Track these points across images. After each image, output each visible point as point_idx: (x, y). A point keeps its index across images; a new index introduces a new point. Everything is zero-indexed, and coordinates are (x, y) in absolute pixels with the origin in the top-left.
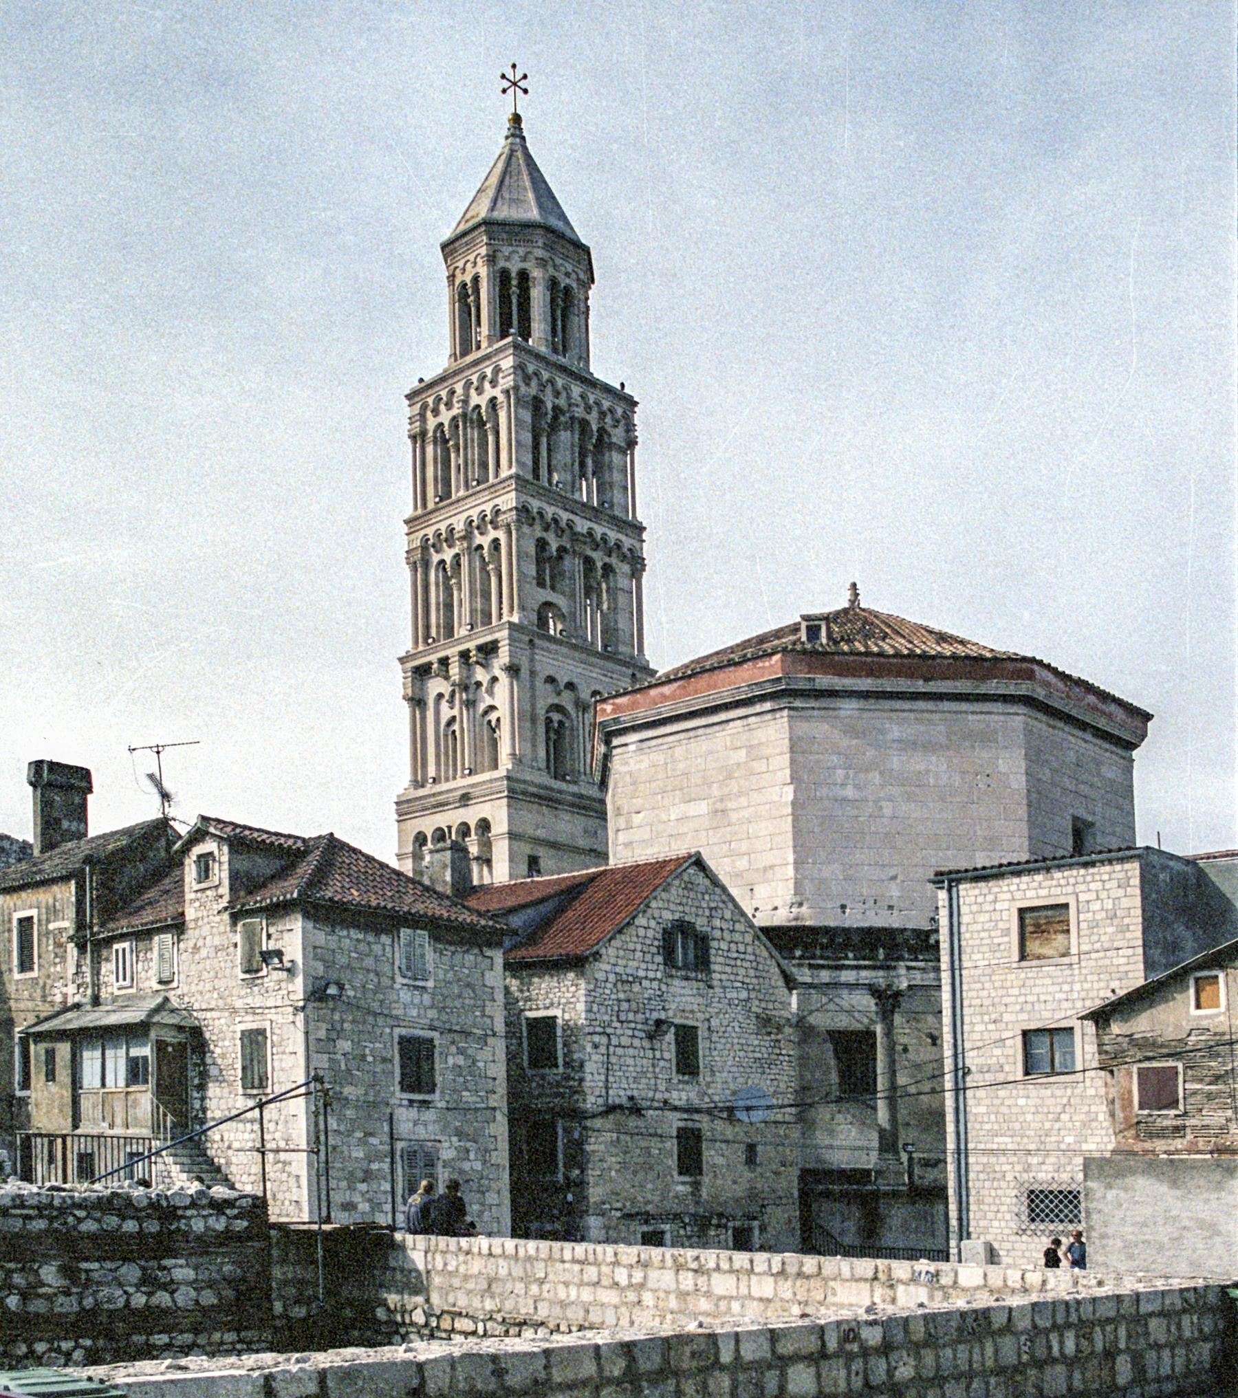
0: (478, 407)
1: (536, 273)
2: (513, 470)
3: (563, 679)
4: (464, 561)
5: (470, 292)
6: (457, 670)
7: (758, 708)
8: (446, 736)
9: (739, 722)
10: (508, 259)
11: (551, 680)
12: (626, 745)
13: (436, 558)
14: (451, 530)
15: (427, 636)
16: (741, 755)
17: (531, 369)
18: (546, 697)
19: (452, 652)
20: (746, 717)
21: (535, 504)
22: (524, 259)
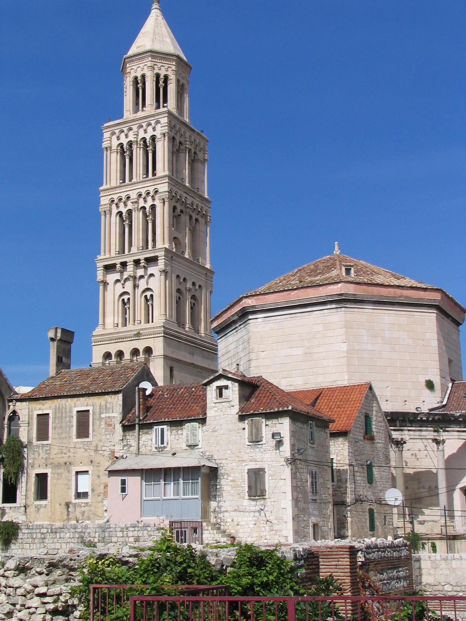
2: (167, 173)
6: (132, 269)
8: (118, 300)
13: (115, 211)
16: (320, 328)
19: (130, 260)
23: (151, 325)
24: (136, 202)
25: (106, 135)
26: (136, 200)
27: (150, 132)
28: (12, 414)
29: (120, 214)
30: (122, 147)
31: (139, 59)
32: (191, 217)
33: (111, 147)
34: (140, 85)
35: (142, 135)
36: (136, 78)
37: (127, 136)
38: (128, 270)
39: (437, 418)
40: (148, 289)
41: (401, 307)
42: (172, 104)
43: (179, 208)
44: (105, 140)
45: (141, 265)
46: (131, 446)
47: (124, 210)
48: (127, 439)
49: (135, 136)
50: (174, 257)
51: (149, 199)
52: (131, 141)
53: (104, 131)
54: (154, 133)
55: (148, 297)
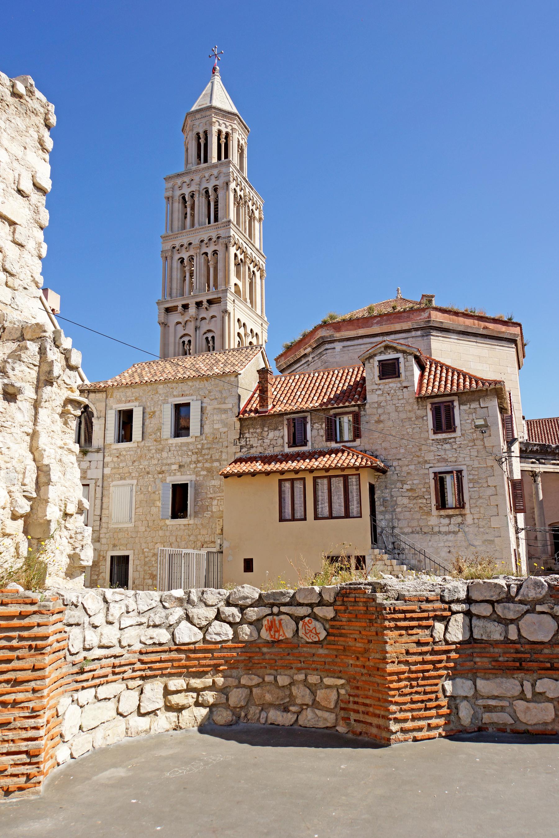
5: (201, 136)
7: (413, 333)
11: (239, 320)
15: (171, 295)
20: (407, 338)
27: (213, 182)
29: (182, 260)
30: (184, 198)
32: (249, 268)
33: (172, 197)
35: (204, 185)
36: (198, 134)
39: (535, 448)
40: (209, 331)
41: (483, 339)
43: (241, 257)
46: (252, 447)
47: (185, 255)
48: (246, 438)
50: (235, 300)
52: (193, 191)
54: (217, 183)
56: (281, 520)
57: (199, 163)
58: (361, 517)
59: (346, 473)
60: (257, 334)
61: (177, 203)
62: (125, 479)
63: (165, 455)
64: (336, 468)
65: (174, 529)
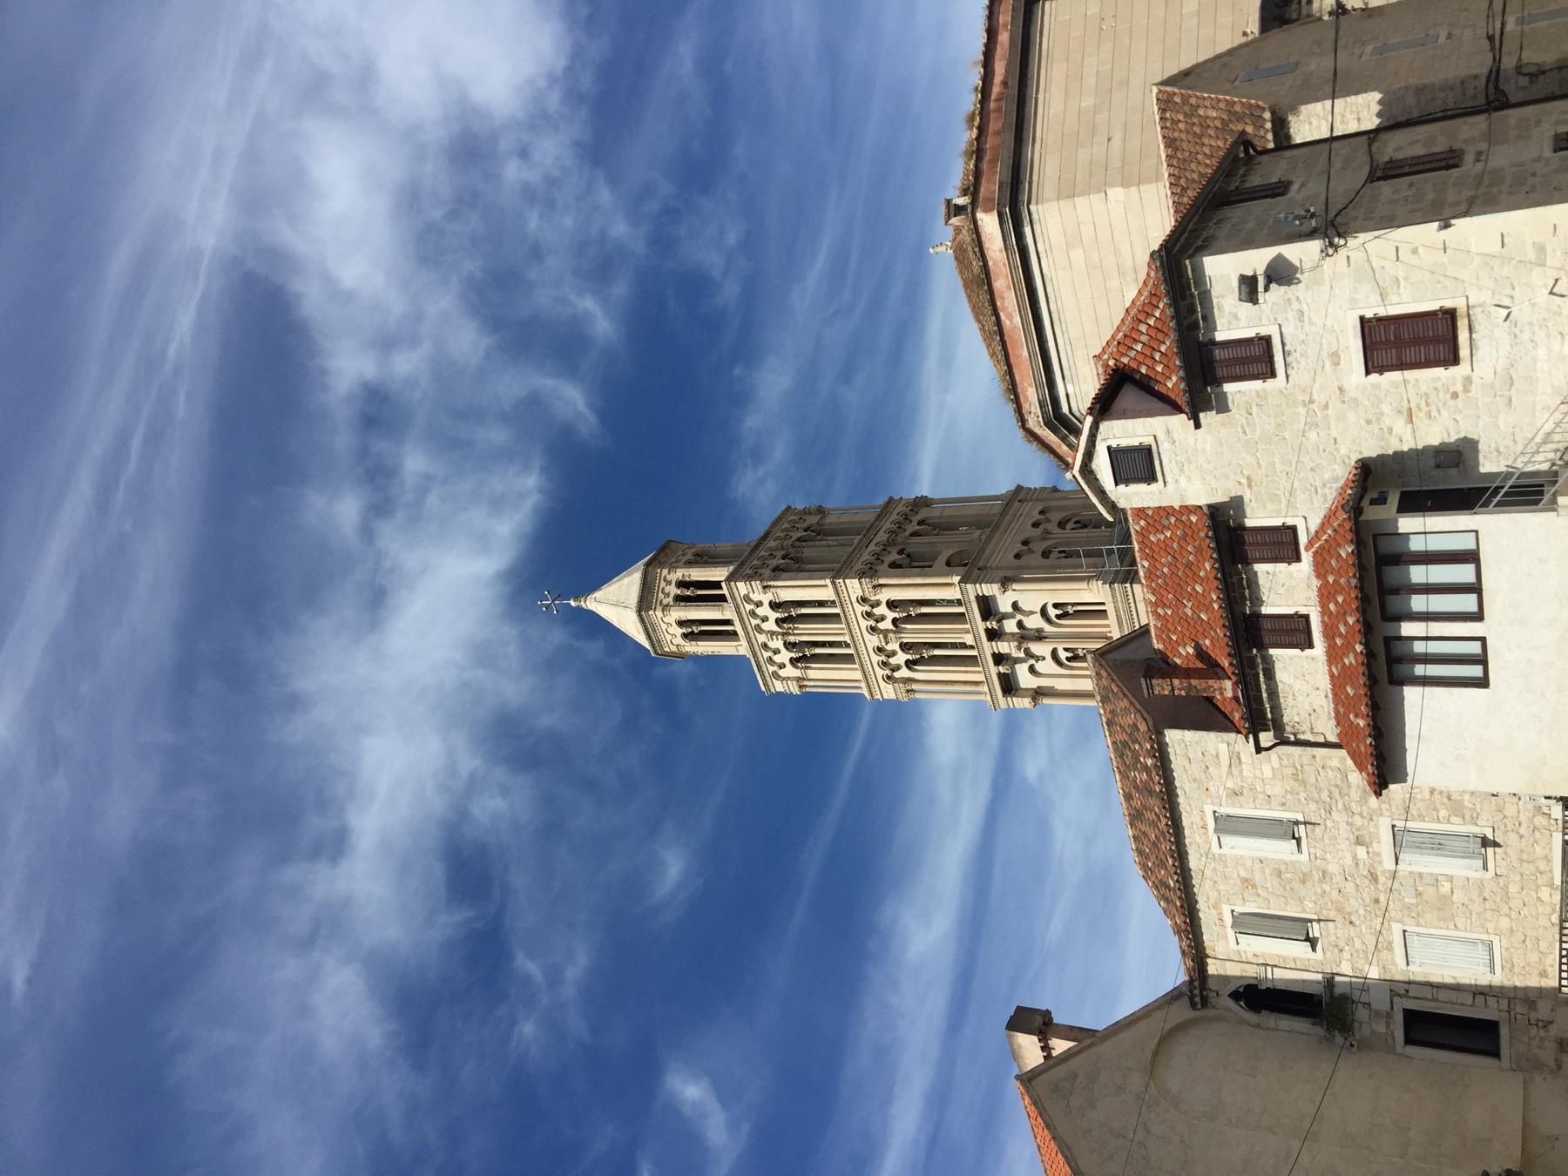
0: (778, 622)
1: (680, 574)
2: (828, 582)
3: (1019, 547)
4: (908, 638)
5: (690, 630)
6: (1005, 644)
8: (1072, 668)
9: (1035, 226)
10: (668, 595)
11: (1017, 556)
12: (1067, 395)
13: (904, 673)
14: (880, 650)
15: (977, 683)
16: (1077, 255)
17: (749, 571)
18: (1036, 559)
19: (988, 648)
21: (859, 566)
22: (669, 583)
23: (1109, 608)
24: (885, 637)
25: (779, 687)
26: (881, 636)
27: (765, 610)
28: (1242, 1003)
31: (654, 631)
32: (914, 534)
33: (799, 679)
34: (696, 629)
35: (770, 625)
36: (685, 636)
37: (777, 652)
38: (1007, 651)
42: (718, 574)
43: (894, 556)
44: (786, 688)
45: (996, 627)
47: (901, 658)
49: (774, 637)
50: (980, 565)
51: (877, 611)
53: (773, 690)
54: (766, 604)
55: (1059, 612)
56: (1483, 682)
57: (735, 633)
58: (1476, 532)
59: (1371, 562)
60: (1042, 512)
61: (809, 671)
62: (1390, 943)
63: (1333, 868)
64: (1361, 587)
65: (1503, 863)
